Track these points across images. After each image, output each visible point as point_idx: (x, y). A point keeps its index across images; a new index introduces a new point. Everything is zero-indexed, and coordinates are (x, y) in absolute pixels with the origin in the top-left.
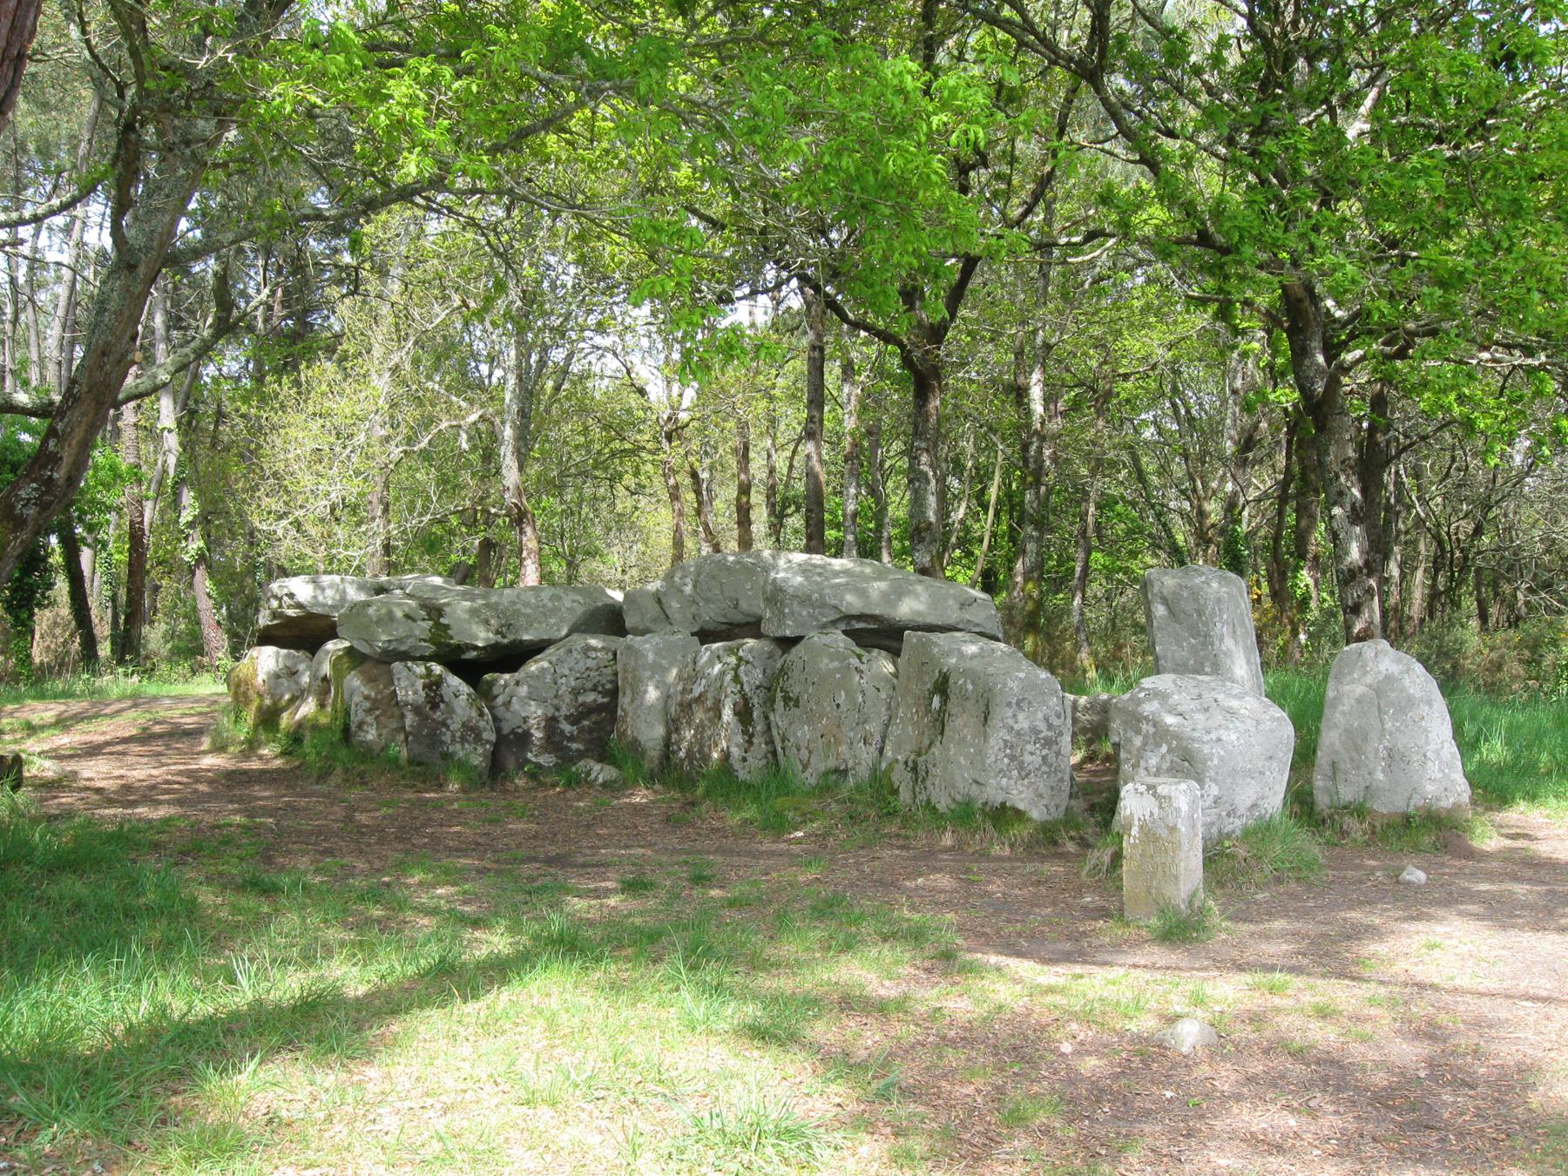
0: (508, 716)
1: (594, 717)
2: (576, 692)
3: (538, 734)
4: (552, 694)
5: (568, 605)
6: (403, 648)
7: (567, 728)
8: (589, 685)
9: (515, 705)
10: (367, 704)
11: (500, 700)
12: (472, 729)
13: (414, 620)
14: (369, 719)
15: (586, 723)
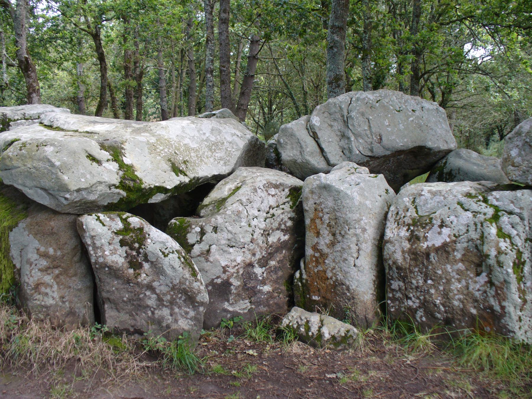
0: (207, 266)
1: (279, 257)
2: (266, 233)
3: (236, 282)
4: (248, 239)
5: (229, 139)
6: (92, 197)
7: (258, 270)
8: (275, 225)
9: (215, 255)
10: (44, 263)
11: (197, 249)
12: (185, 292)
13: (99, 162)
14: (48, 279)
15: (273, 263)
